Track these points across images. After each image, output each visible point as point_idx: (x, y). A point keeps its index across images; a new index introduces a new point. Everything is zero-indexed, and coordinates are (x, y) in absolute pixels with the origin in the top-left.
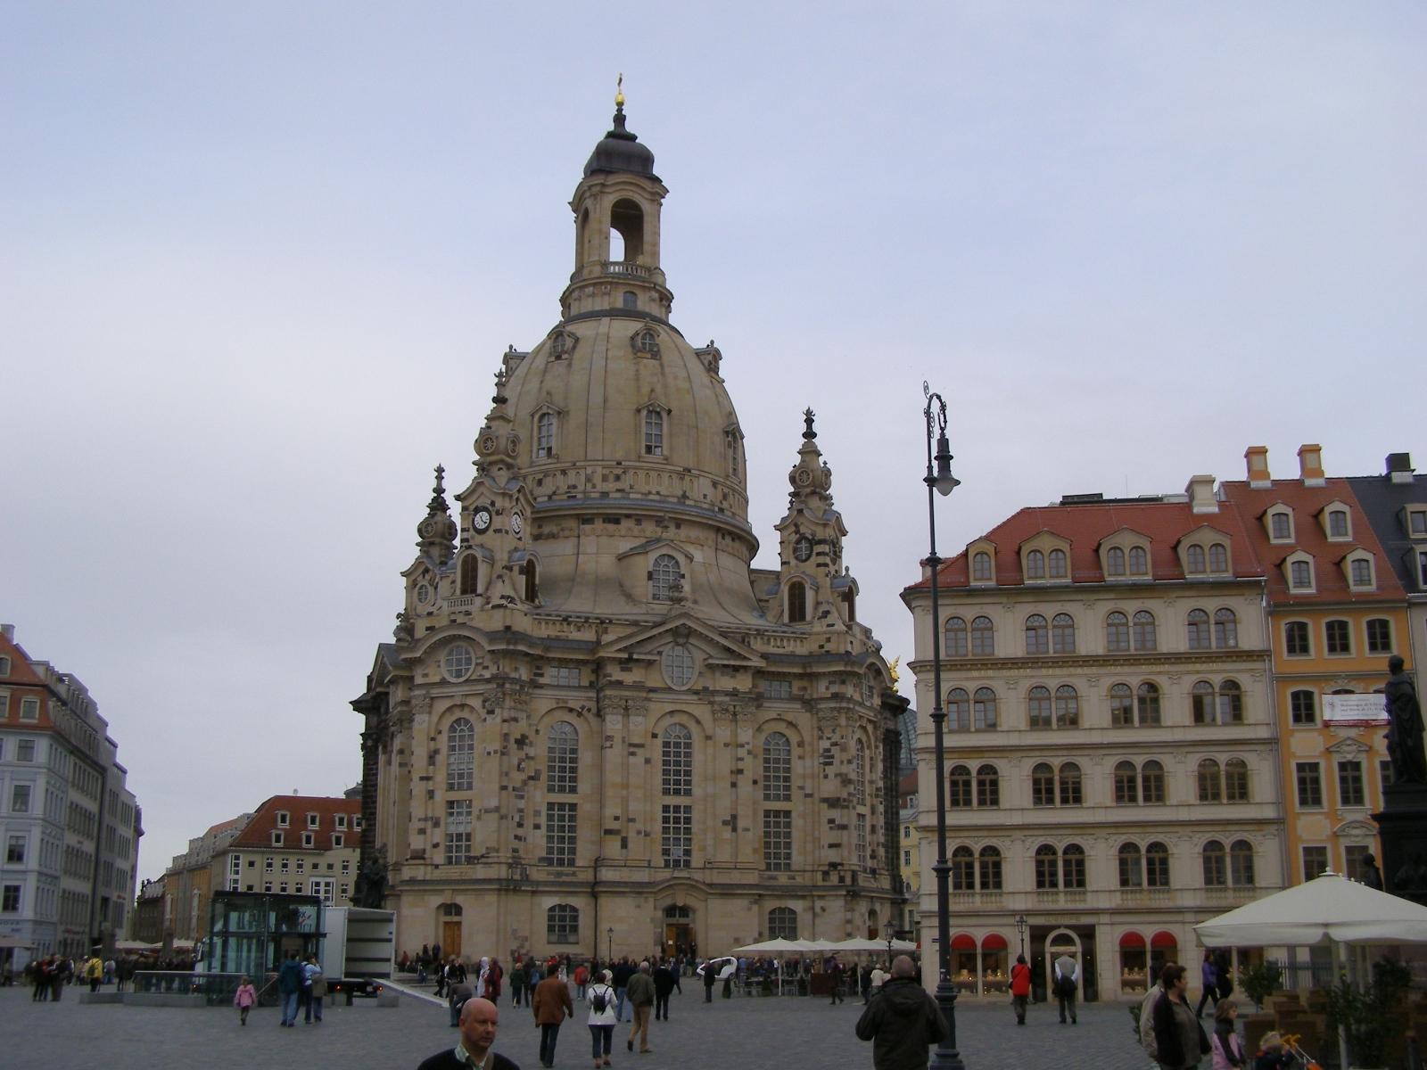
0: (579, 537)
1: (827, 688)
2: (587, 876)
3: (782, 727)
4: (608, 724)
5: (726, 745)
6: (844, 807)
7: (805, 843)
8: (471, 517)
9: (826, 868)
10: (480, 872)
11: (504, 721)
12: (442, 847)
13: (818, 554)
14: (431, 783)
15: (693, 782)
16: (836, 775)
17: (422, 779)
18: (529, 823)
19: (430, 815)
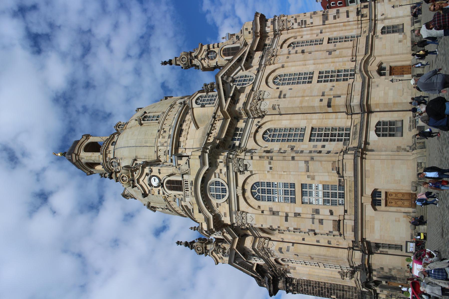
0: (186, 149)
1: (269, 27)
2: (357, 118)
3: (285, 45)
4: (266, 107)
5: (288, 57)
6: (327, 12)
7: (345, 30)
8: (153, 188)
9: (360, 17)
10: (349, 173)
11: (252, 158)
12: (333, 208)
13: (214, 48)
14: (290, 215)
15: (306, 71)
16: (311, 17)
17: (286, 220)
18: (319, 149)
19: (310, 216)
